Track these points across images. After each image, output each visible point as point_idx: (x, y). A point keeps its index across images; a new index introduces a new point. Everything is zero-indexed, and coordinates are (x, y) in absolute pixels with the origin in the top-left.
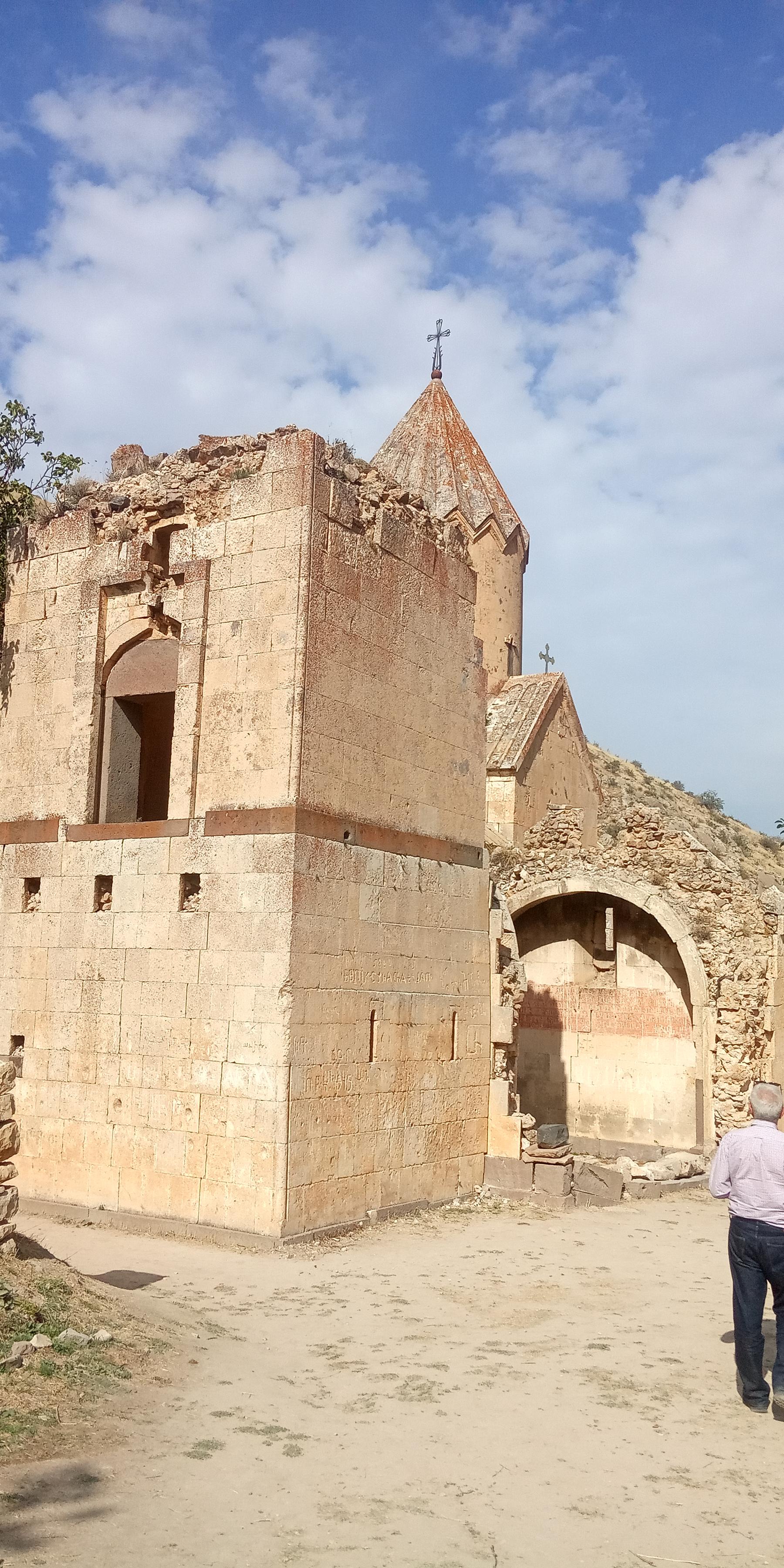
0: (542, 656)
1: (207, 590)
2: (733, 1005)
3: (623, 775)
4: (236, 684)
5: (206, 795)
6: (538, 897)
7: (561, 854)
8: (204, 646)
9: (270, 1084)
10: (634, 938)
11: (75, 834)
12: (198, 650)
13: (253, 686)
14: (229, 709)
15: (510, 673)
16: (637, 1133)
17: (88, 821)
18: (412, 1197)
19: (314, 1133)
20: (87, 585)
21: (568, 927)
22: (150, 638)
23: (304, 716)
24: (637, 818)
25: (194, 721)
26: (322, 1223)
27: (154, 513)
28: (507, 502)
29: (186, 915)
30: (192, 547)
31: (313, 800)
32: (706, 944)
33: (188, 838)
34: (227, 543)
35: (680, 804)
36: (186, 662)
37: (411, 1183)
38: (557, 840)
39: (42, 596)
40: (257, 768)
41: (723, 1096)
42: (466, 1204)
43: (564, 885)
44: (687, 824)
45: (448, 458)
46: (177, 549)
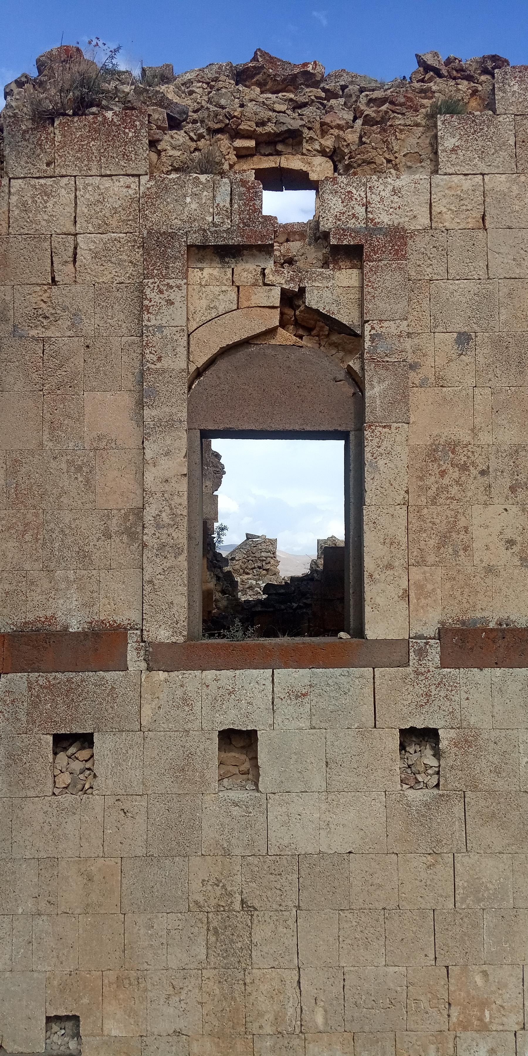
4: (474, 430)
5: (429, 601)
11: (160, 658)
14: (464, 468)
22: (273, 342)
27: (252, 143)
30: (366, 205)
33: (409, 670)
34: (435, 210)
38: (260, 568)
39: (46, 245)
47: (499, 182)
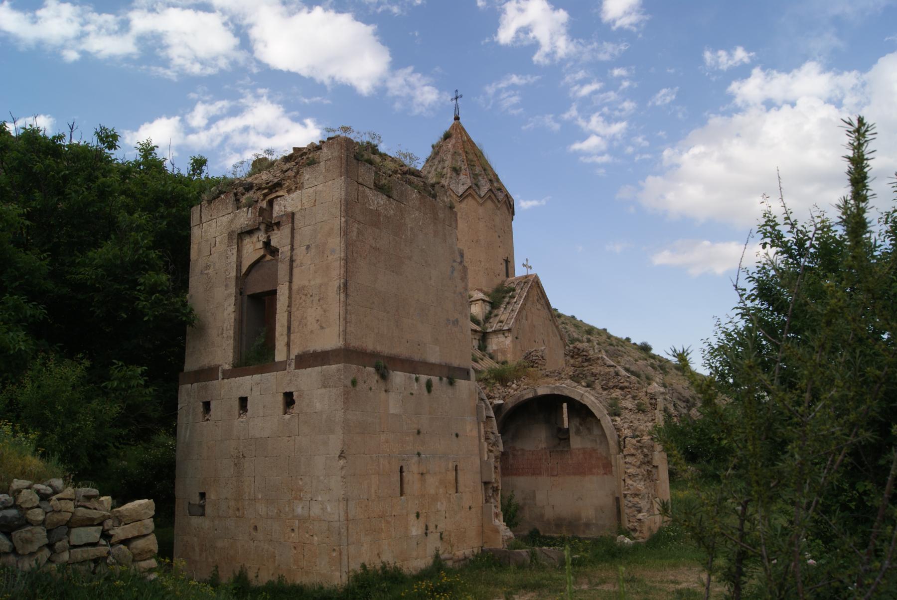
0: (524, 265)
1: (293, 229)
2: (633, 451)
8: (292, 261)
10: (578, 420)
11: (228, 375)
12: (288, 263)
13: (318, 281)
14: (306, 295)
15: (507, 276)
17: (234, 367)
20: (230, 235)
23: (347, 295)
24: (576, 350)
25: (287, 304)
27: (266, 191)
29: (287, 416)
31: (354, 343)
32: (618, 419)
36: (282, 269)
40: (322, 328)
41: (630, 505)
43: (535, 391)
46: (277, 210)
47: (320, 187)
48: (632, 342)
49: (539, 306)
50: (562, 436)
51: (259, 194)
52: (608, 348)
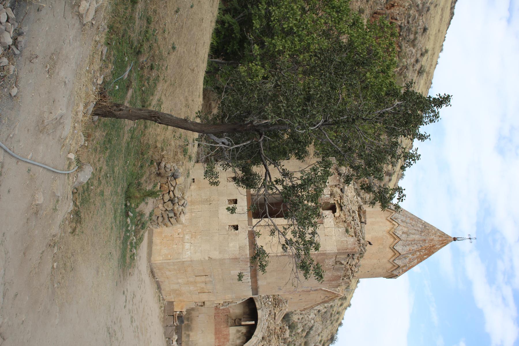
3: (340, 303)
6: (255, 301)
7: (271, 306)
9: (187, 256)
16: (185, 335)
18: (162, 287)
19: (176, 267)
21: (247, 310)
23: (280, 256)
24: (284, 330)
26: (154, 270)
28: (406, 271)
29: (227, 227)
35: (330, 327)
37: (166, 287)
42: (161, 299)
44: (319, 331)
45: (420, 248)
47: (334, 238)
48: (339, 328)
49: (323, 297)
50: (237, 323)
51: (338, 198)
52: (329, 314)
